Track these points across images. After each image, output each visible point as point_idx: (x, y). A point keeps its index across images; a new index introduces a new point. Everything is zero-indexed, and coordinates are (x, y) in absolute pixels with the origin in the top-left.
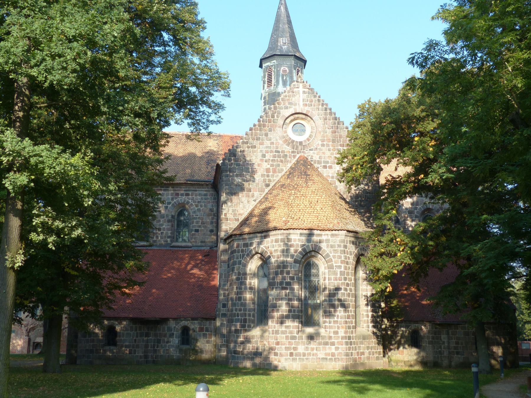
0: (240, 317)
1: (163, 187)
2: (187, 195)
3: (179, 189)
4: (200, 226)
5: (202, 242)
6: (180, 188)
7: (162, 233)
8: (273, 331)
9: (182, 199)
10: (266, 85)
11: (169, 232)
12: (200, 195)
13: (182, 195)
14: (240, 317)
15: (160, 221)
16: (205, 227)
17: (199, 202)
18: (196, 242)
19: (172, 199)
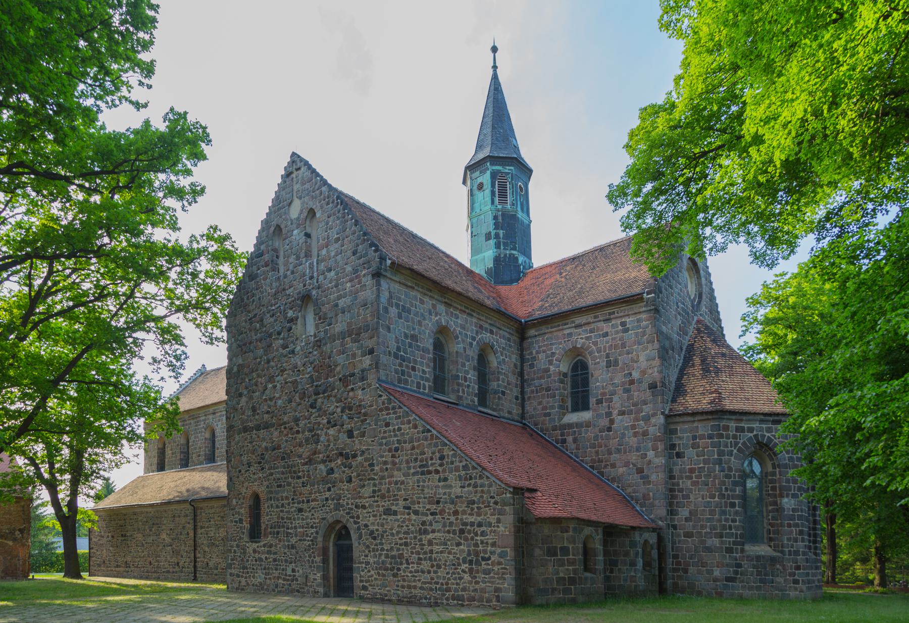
0: (733, 531)
1: (467, 308)
2: (492, 332)
3: (483, 318)
4: (506, 387)
5: (509, 413)
6: (486, 317)
7: (468, 386)
8: (790, 551)
9: (486, 336)
10: (497, 199)
11: (477, 387)
12: (504, 337)
13: (486, 330)
14: (733, 531)
15: (464, 365)
16: (511, 390)
17: (504, 348)
18: (503, 410)
19: (477, 333)
